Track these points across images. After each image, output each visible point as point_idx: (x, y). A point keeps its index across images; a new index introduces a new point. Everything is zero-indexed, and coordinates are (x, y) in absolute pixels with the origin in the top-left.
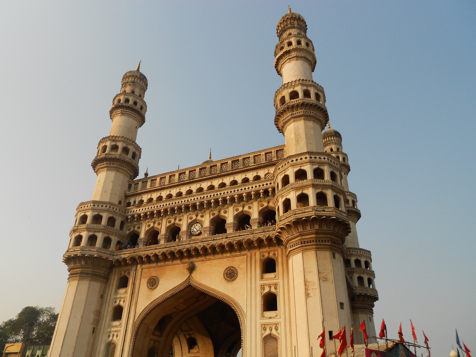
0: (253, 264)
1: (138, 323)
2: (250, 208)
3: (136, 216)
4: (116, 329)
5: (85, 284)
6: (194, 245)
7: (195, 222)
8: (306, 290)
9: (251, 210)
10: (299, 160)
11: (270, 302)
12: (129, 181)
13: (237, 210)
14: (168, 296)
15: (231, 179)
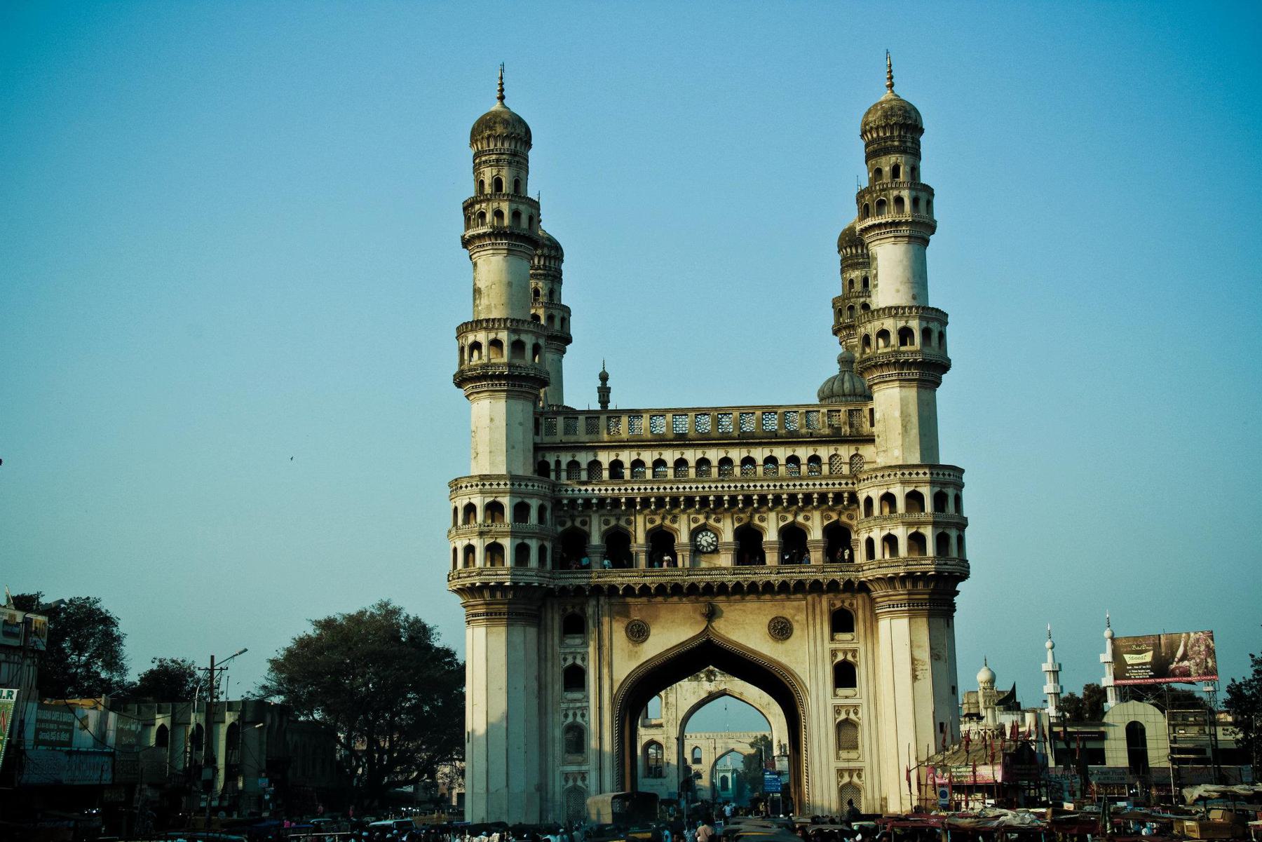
0: (818, 618)
1: (620, 697)
2: (807, 518)
3: (580, 501)
4: (578, 705)
5: (518, 631)
6: (719, 579)
7: (703, 528)
8: (914, 670)
9: (809, 523)
10: (914, 476)
11: (845, 675)
12: (535, 413)
13: (784, 519)
14: (670, 655)
15: (766, 452)
